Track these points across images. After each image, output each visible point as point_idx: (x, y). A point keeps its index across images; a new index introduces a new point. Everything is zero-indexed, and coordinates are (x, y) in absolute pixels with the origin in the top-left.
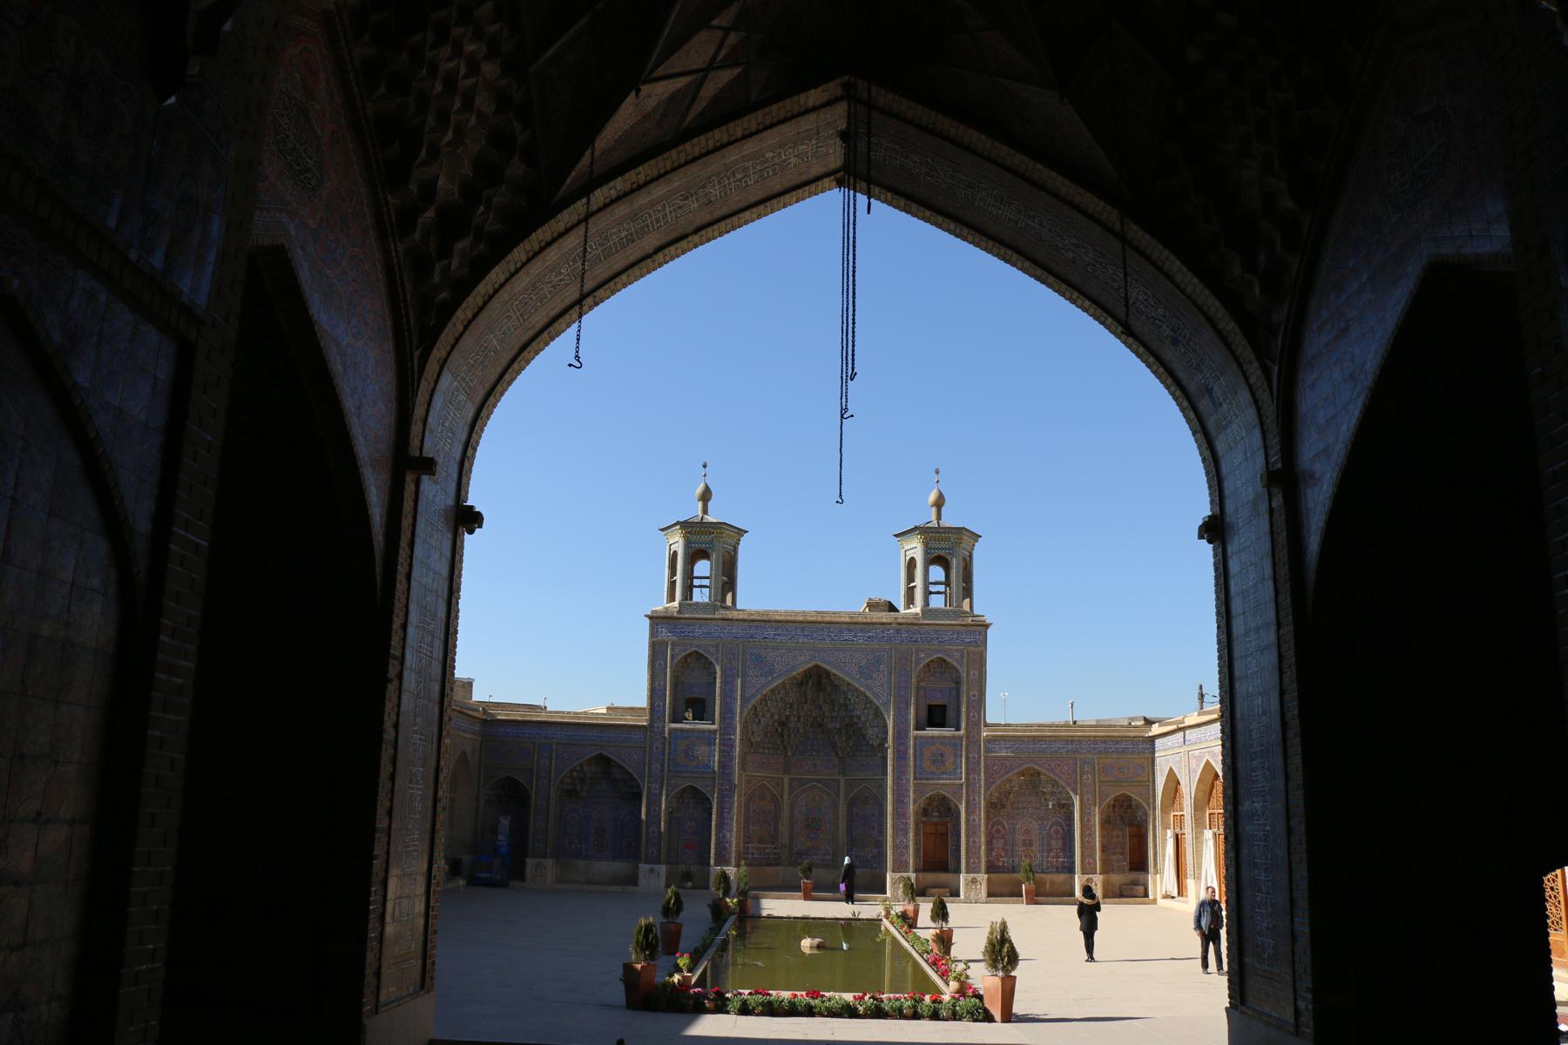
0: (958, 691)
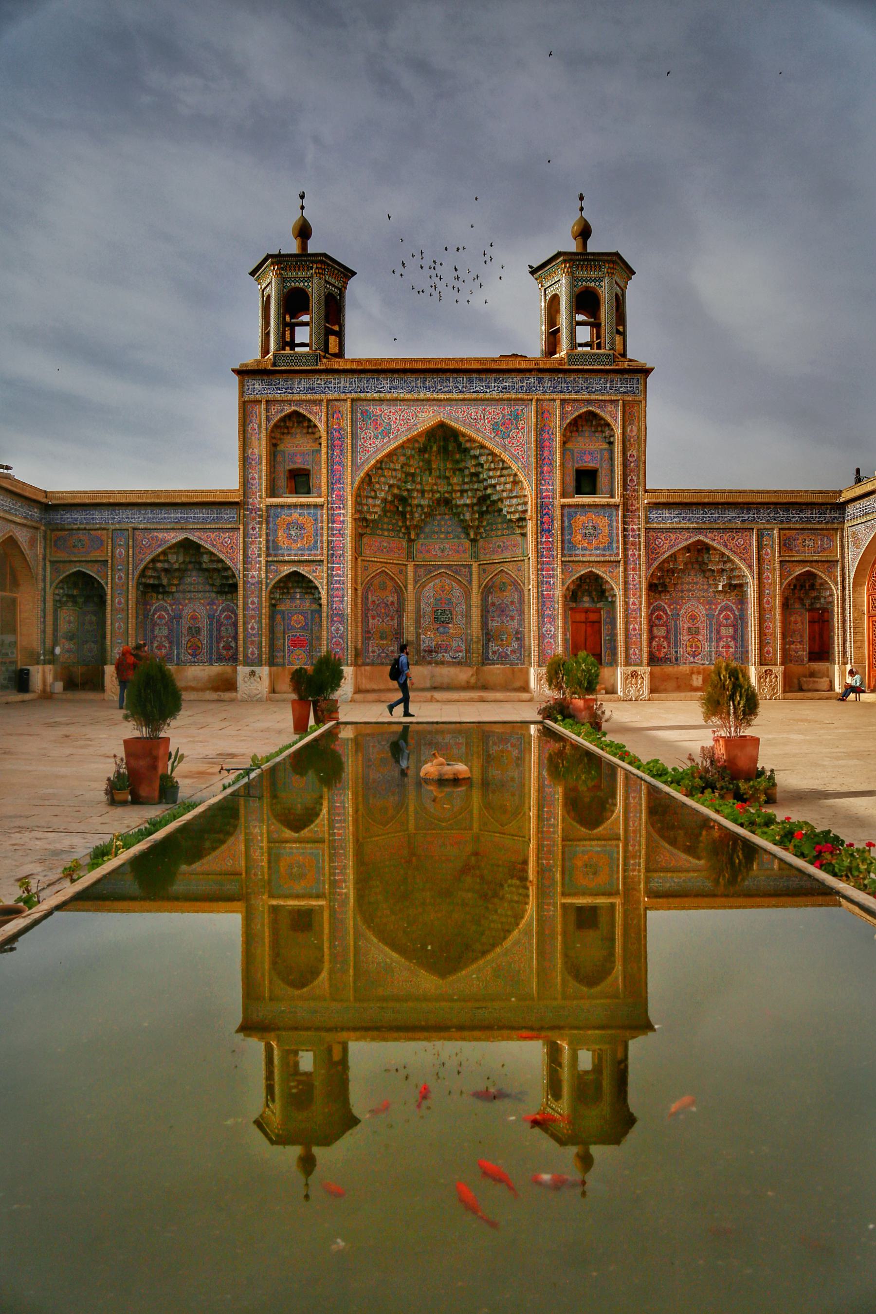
0: (612, 452)
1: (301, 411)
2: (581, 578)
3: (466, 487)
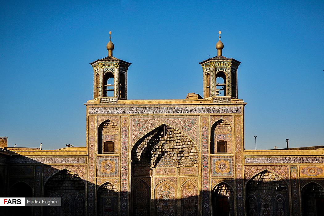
3: (175, 147)
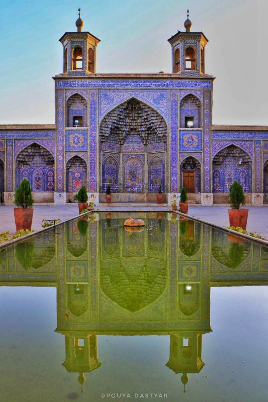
0: (199, 111)
1: (79, 93)
2: (187, 159)
